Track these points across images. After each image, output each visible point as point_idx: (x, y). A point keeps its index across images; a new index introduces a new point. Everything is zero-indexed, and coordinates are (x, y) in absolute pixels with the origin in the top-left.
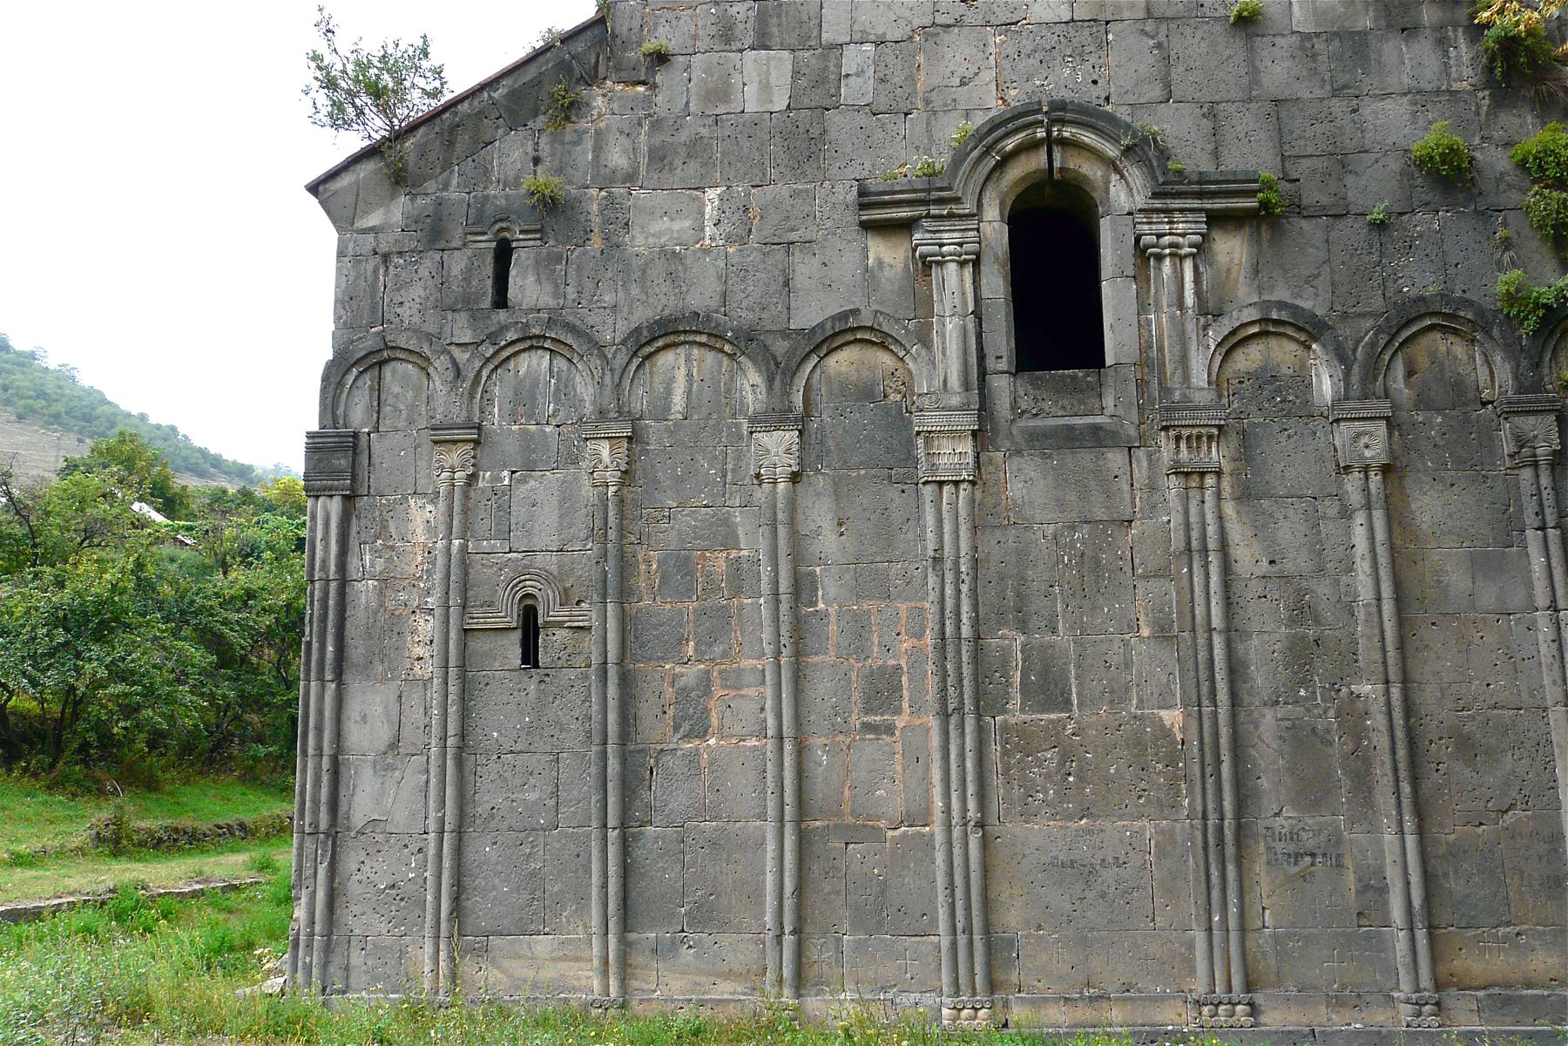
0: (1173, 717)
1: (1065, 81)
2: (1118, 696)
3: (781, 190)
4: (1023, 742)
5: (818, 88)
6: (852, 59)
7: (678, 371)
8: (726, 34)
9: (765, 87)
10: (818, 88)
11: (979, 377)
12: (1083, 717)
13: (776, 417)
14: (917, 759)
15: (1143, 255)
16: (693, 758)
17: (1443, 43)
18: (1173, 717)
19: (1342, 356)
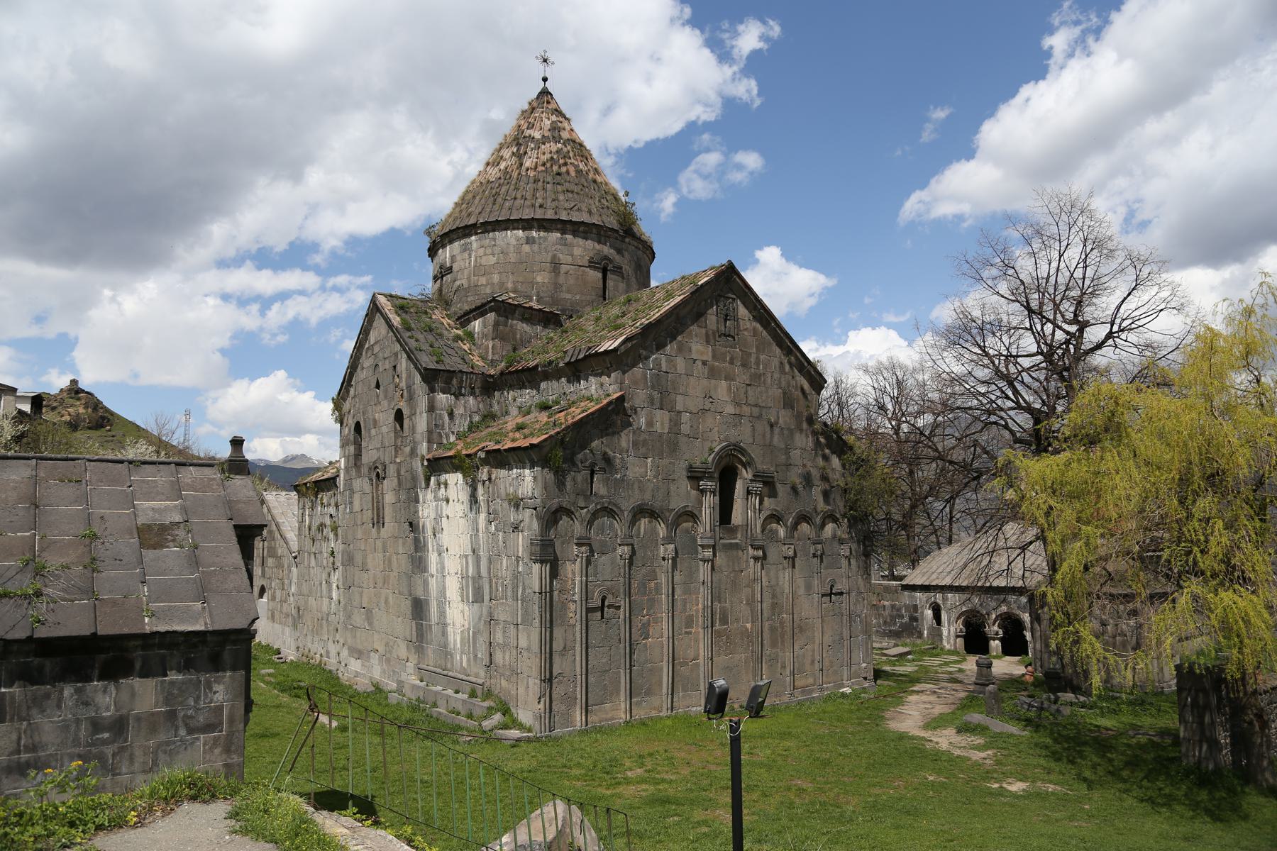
0: (749, 626)
1: (733, 435)
2: (738, 620)
3: (666, 461)
4: (719, 634)
5: (675, 423)
6: (685, 417)
7: (644, 523)
8: (652, 402)
9: (662, 424)
10: (675, 423)
11: (712, 530)
12: (733, 626)
13: (669, 540)
14: (697, 640)
15: (748, 492)
16: (645, 645)
17: (807, 436)
18: (749, 626)
19: (786, 526)
